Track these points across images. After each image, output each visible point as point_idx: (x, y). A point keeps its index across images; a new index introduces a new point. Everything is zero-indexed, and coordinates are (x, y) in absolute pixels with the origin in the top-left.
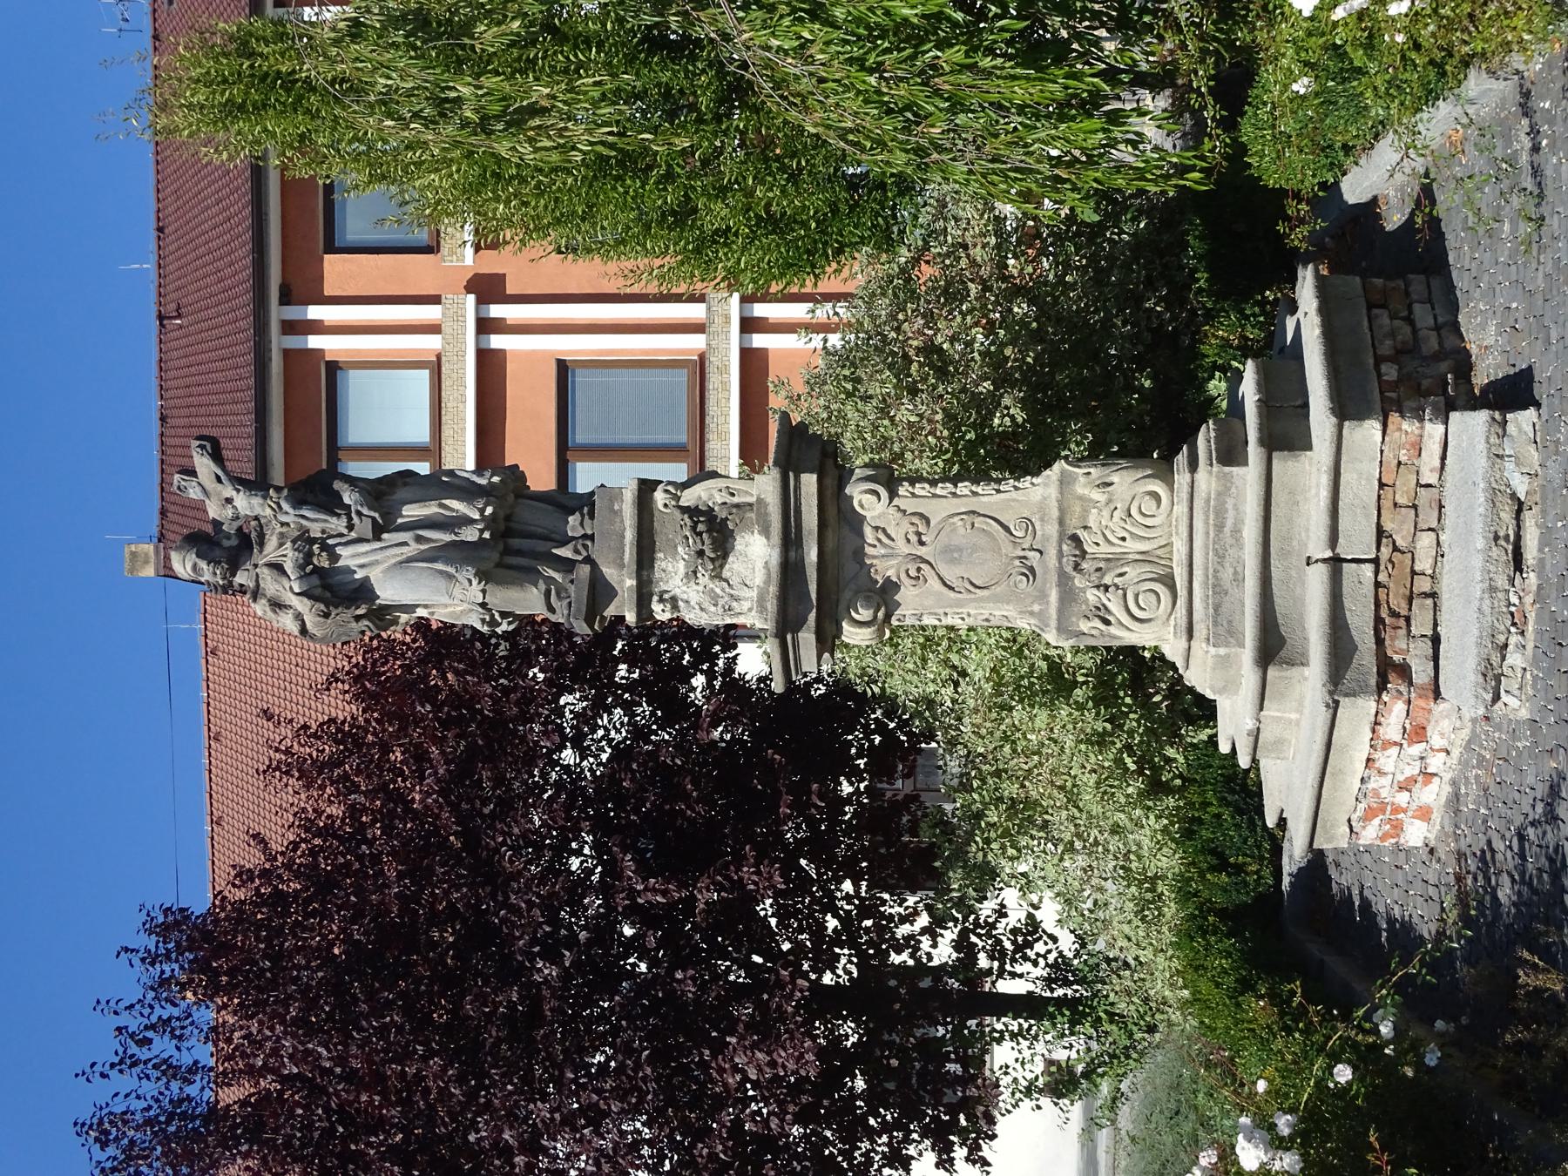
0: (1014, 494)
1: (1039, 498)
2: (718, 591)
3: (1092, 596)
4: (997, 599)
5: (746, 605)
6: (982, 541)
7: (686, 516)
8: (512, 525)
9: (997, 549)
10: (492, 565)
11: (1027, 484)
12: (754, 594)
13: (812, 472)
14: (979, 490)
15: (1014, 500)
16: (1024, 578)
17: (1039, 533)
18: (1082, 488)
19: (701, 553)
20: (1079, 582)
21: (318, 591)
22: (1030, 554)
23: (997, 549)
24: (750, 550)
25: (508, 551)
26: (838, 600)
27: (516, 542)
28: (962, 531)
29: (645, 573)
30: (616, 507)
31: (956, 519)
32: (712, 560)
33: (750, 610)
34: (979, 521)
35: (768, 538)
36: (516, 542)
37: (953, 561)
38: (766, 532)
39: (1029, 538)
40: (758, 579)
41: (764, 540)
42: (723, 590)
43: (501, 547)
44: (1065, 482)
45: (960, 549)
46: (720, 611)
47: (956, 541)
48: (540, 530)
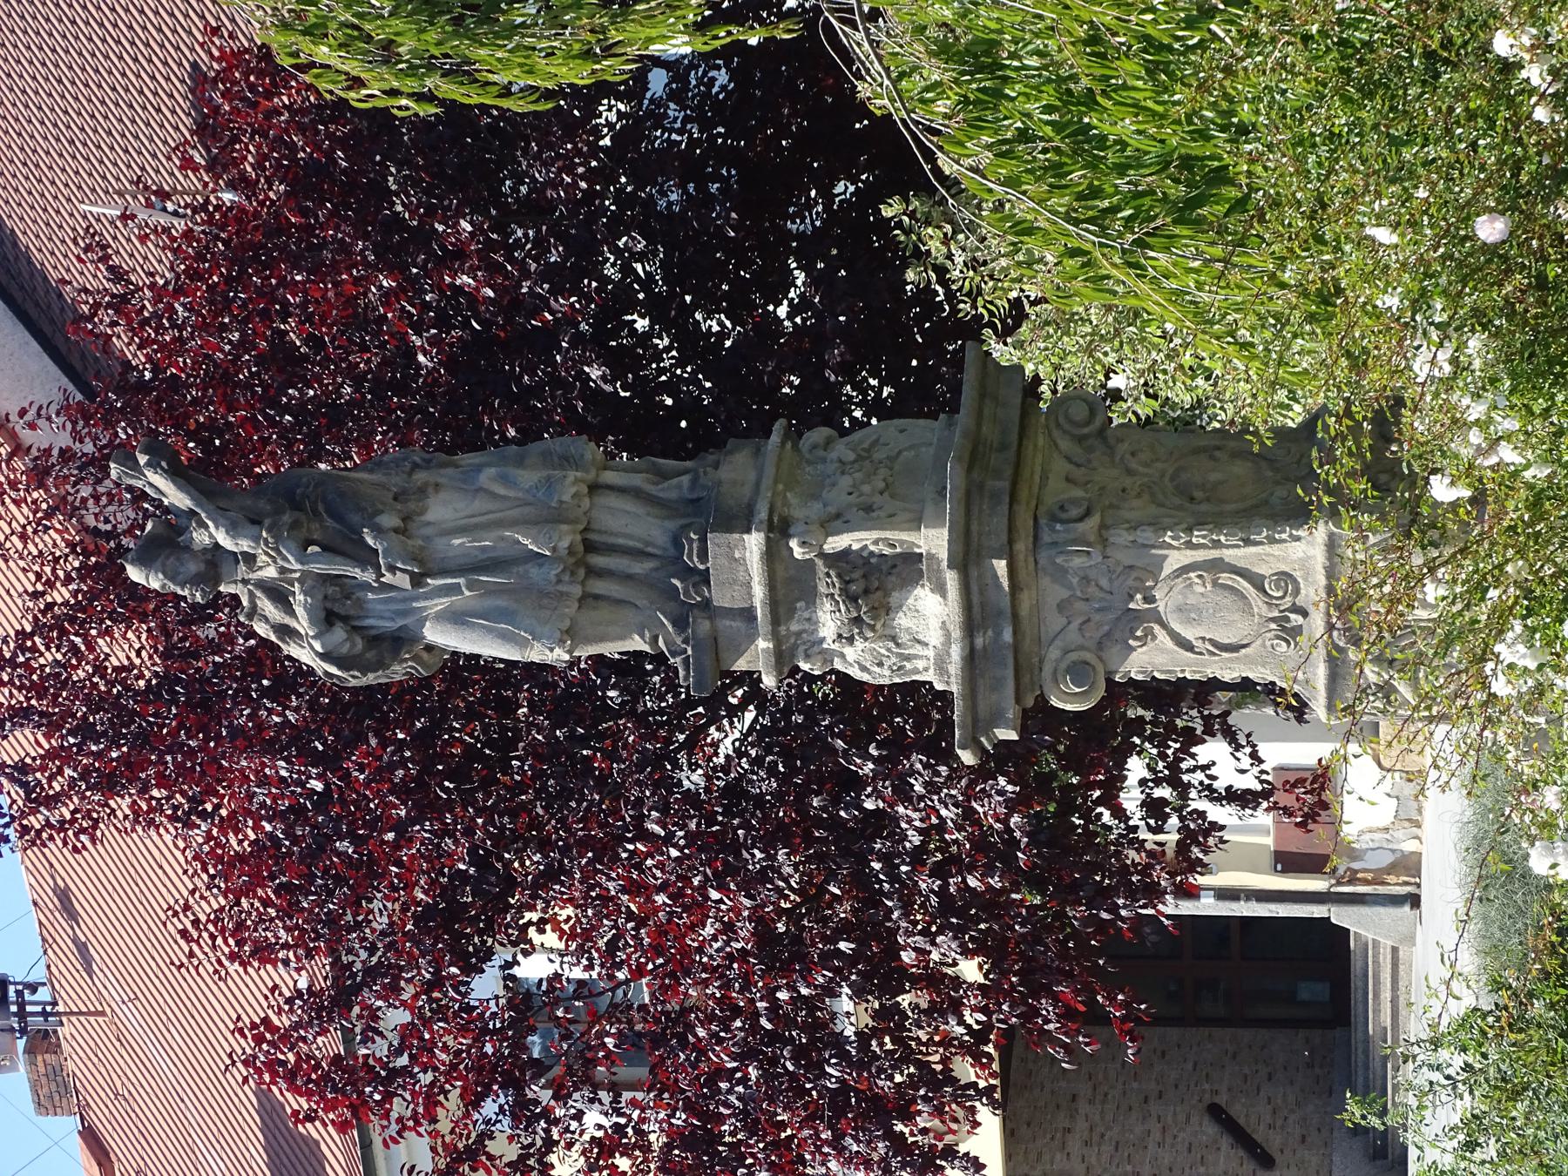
0: (1267, 548)
1: (1301, 555)
2: (883, 651)
3: (1371, 674)
4: (1250, 661)
5: (920, 664)
6: (1227, 600)
7: (832, 573)
8: (593, 537)
9: (1247, 608)
10: (576, 605)
11: (1284, 536)
12: (931, 653)
13: (1000, 558)
14: (1222, 538)
15: (1268, 555)
16: (1284, 644)
17: (1303, 592)
18: (1354, 553)
19: (857, 621)
20: (1353, 655)
21: (345, 649)
22: (1293, 616)
23: (1247, 608)
24: (920, 605)
25: (593, 572)
26: (1041, 661)
27: (599, 561)
28: (1200, 589)
29: (783, 629)
30: (737, 555)
31: (1192, 575)
32: (872, 628)
33: (926, 669)
34: (1225, 579)
35: (944, 595)
36: (599, 561)
37: (1189, 622)
38: (940, 589)
39: (1288, 599)
40: (934, 638)
41: (938, 598)
42: (889, 650)
43: (582, 572)
44: (1332, 545)
45: (1199, 611)
46: (887, 673)
47: (1192, 600)
48: (631, 543)
